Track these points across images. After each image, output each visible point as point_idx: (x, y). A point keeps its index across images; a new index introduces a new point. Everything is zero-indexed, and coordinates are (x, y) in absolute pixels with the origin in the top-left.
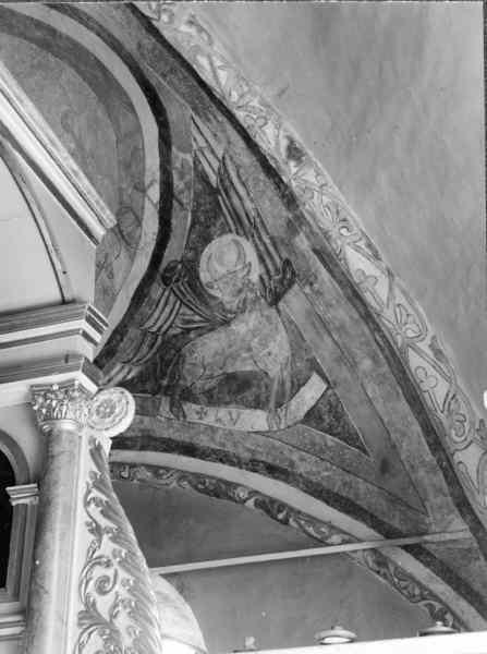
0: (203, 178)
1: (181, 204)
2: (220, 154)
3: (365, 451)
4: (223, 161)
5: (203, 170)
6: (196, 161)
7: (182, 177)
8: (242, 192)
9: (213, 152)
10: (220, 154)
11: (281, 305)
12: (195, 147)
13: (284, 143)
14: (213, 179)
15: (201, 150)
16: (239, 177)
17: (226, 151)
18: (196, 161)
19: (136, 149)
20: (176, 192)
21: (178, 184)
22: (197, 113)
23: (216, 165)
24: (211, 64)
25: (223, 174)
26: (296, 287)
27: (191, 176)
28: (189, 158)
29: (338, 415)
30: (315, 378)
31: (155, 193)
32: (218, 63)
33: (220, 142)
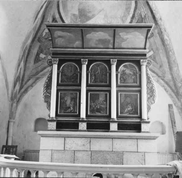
0: (141, 16)
1: (135, 18)
2: (146, 13)
3: (157, 64)
4: (146, 14)
5: (141, 15)
6: (141, 13)
7: (137, 14)
8: (148, 20)
9: (144, 12)
10: (146, 13)
11: (150, 39)
12: (141, 11)
13: (160, 17)
14: (143, 17)
15: (142, 12)
16: (148, 18)
17: (147, 13)
18: (141, 13)
19: (129, 7)
20: (135, 16)
21: (136, 15)
22: (144, 6)
23: (144, 14)
24: (152, 3)
25: (145, 16)
26: (153, 38)
27: (139, 14)
28: (140, 12)
29: (155, 58)
30: (152, 51)
31: (131, 15)
32: (153, 3)
33: (146, 11)
